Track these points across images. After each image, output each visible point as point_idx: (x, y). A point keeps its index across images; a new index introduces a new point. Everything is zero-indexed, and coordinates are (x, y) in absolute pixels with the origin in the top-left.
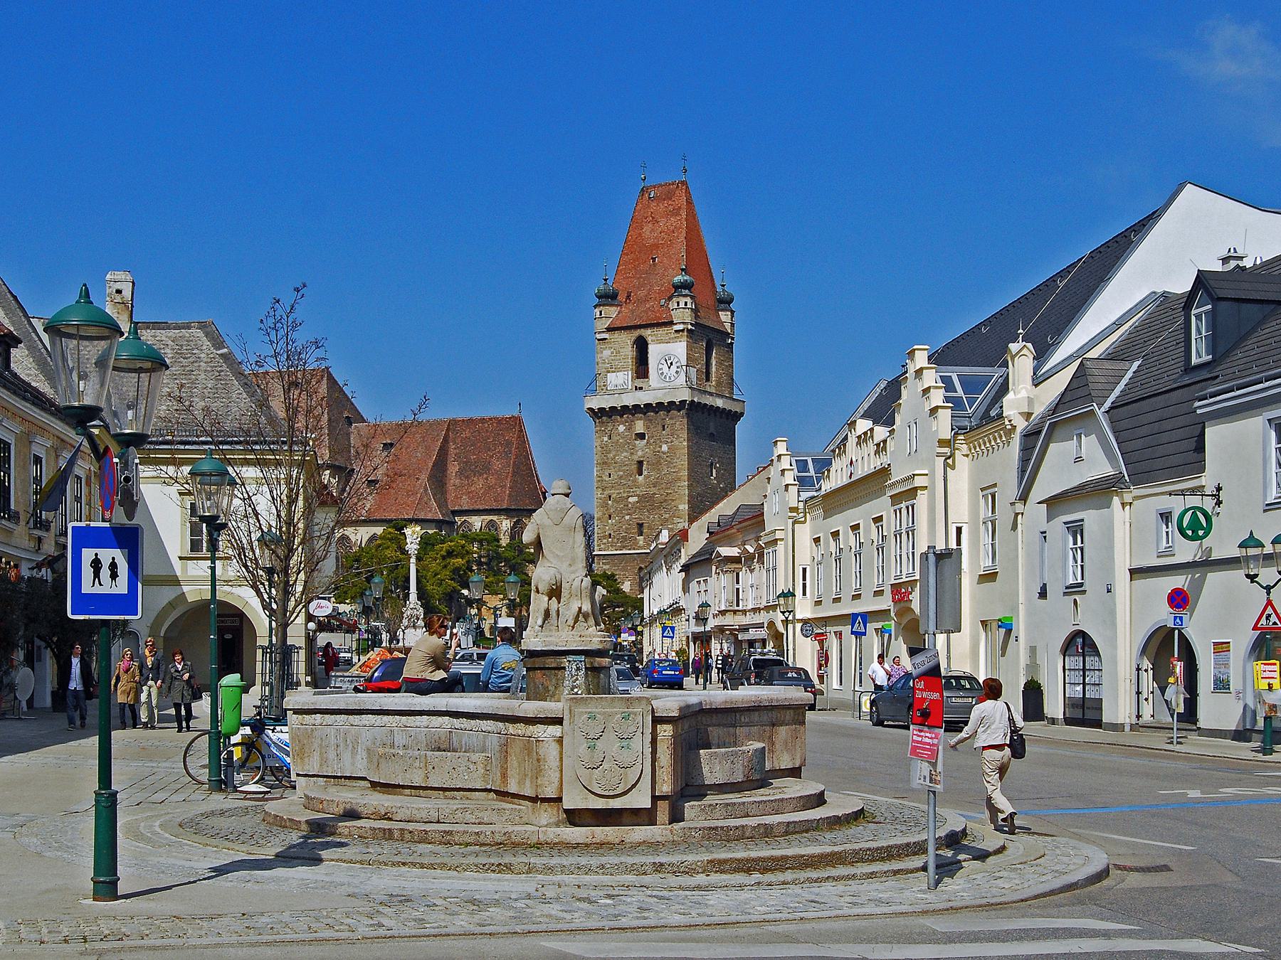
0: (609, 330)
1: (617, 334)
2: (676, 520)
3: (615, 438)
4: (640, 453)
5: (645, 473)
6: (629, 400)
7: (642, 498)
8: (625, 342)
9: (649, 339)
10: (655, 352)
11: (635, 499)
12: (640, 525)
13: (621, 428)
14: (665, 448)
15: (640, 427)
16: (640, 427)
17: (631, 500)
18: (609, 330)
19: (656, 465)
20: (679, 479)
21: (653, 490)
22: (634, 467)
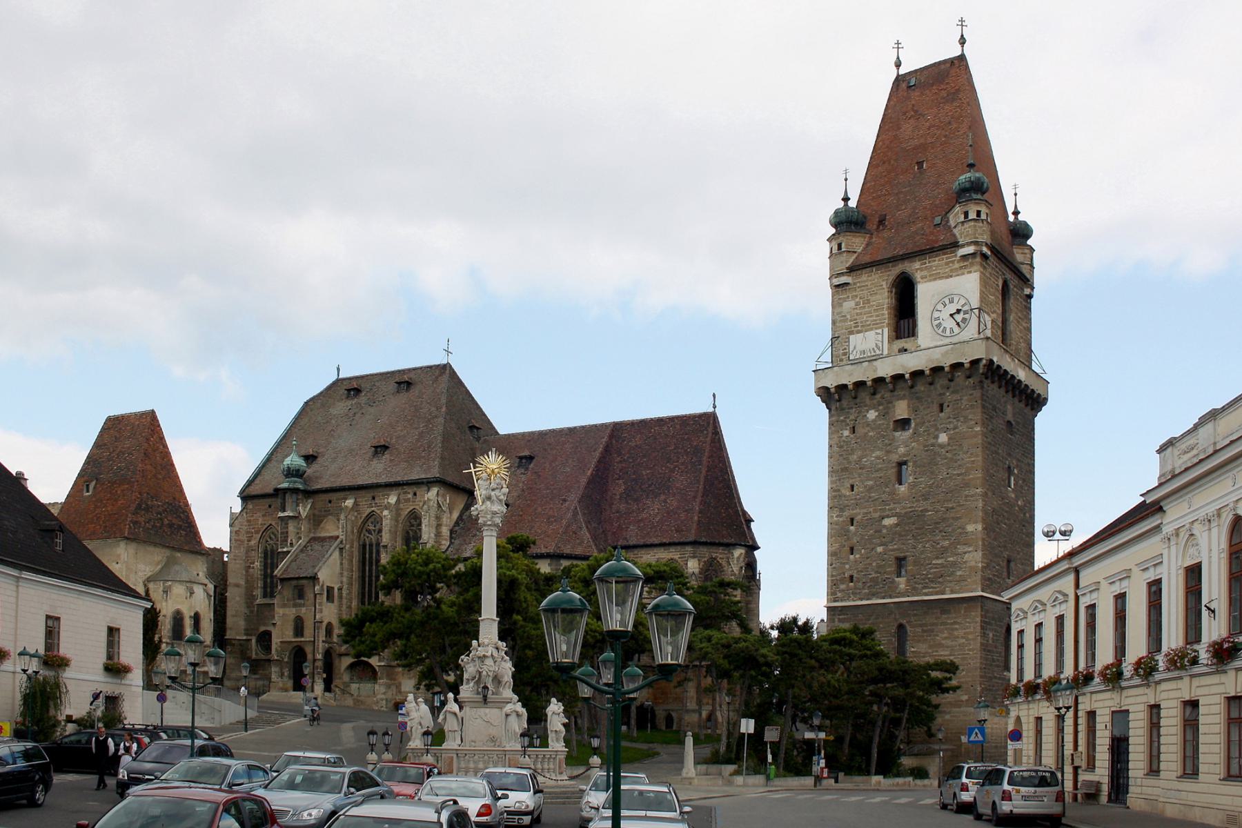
2: (961, 549)
3: (860, 431)
4: (902, 450)
6: (886, 369)
7: (904, 519)
10: (926, 294)
13: (872, 415)
15: (901, 409)
17: (887, 522)
18: (852, 270)
20: (967, 485)
22: (892, 472)
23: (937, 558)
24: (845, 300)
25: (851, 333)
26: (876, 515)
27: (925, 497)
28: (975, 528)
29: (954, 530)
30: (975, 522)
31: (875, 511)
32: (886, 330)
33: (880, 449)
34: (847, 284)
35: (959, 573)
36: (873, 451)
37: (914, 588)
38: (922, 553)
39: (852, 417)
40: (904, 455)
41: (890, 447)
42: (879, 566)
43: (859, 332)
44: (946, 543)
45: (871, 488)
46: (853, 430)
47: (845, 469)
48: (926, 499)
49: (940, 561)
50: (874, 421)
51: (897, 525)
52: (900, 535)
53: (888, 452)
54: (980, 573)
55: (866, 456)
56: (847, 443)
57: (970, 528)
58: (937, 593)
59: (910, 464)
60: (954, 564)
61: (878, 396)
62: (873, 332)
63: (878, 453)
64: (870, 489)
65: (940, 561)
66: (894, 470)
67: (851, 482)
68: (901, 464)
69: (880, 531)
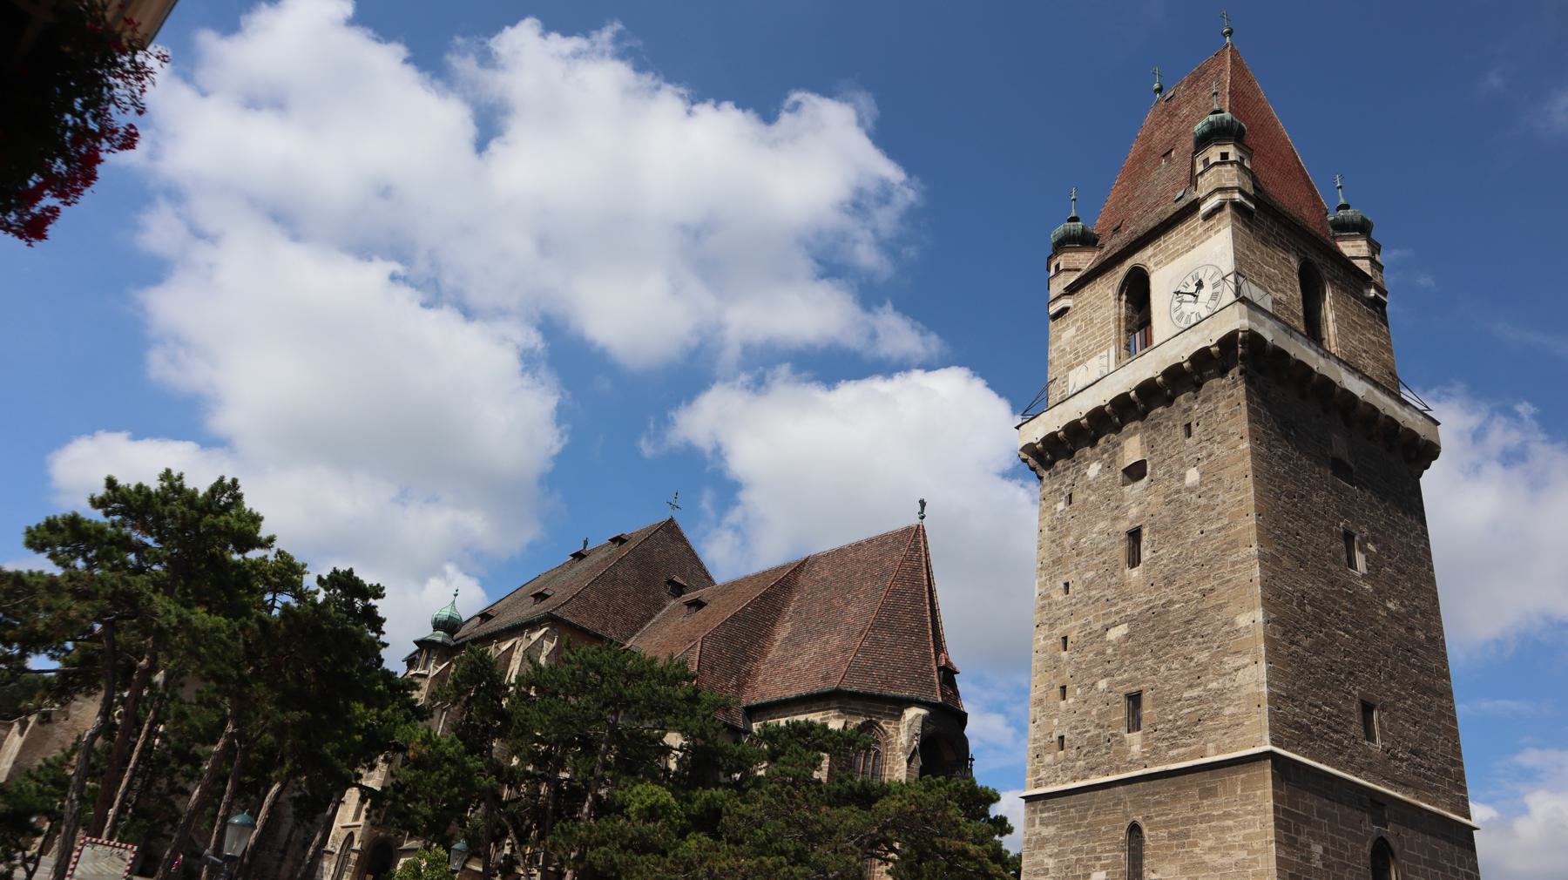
0: (1071, 290)
1: (1087, 293)
2: (1231, 662)
3: (1078, 497)
4: (1134, 511)
5: (1146, 555)
8: (1105, 298)
9: (1151, 266)
11: (1122, 630)
12: (1135, 700)
13: (1094, 470)
14: (1192, 476)
16: (1132, 449)
17: (1115, 634)
18: (1071, 290)
19: (1172, 529)
20: (1233, 545)
21: (1171, 593)
22: (1121, 550)
23: (1191, 686)
24: (1064, 330)
25: (1071, 368)
26: (1098, 626)
27: (1169, 582)
28: (1252, 619)
29: (1216, 631)
31: (1097, 619)
33: (1104, 518)
34: (1065, 310)
35: (1227, 711)
36: (1094, 524)
37: (1155, 750)
38: (1166, 680)
39: (1068, 481)
40: (1139, 518)
41: (1118, 512)
42: (1101, 715)
44: (1204, 657)
45: (1092, 582)
47: (1057, 561)
48: (1170, 583)
49: (1195, 693)
51: (1128, 636)
52: (1134, 654)
53: (1115, 519)
54: (1265, 707)
58: (1192, 756)
59: (1145, 531)
60: (1220, 694)
61: (1101, 441)
62: (1096, 359)
63: (1102, 525)
64: (1089, 585)
65: (1195, 693)
66: (1125, 545)
67: (1065, 578)
68: (1135, 535)
69: (1103, 653)
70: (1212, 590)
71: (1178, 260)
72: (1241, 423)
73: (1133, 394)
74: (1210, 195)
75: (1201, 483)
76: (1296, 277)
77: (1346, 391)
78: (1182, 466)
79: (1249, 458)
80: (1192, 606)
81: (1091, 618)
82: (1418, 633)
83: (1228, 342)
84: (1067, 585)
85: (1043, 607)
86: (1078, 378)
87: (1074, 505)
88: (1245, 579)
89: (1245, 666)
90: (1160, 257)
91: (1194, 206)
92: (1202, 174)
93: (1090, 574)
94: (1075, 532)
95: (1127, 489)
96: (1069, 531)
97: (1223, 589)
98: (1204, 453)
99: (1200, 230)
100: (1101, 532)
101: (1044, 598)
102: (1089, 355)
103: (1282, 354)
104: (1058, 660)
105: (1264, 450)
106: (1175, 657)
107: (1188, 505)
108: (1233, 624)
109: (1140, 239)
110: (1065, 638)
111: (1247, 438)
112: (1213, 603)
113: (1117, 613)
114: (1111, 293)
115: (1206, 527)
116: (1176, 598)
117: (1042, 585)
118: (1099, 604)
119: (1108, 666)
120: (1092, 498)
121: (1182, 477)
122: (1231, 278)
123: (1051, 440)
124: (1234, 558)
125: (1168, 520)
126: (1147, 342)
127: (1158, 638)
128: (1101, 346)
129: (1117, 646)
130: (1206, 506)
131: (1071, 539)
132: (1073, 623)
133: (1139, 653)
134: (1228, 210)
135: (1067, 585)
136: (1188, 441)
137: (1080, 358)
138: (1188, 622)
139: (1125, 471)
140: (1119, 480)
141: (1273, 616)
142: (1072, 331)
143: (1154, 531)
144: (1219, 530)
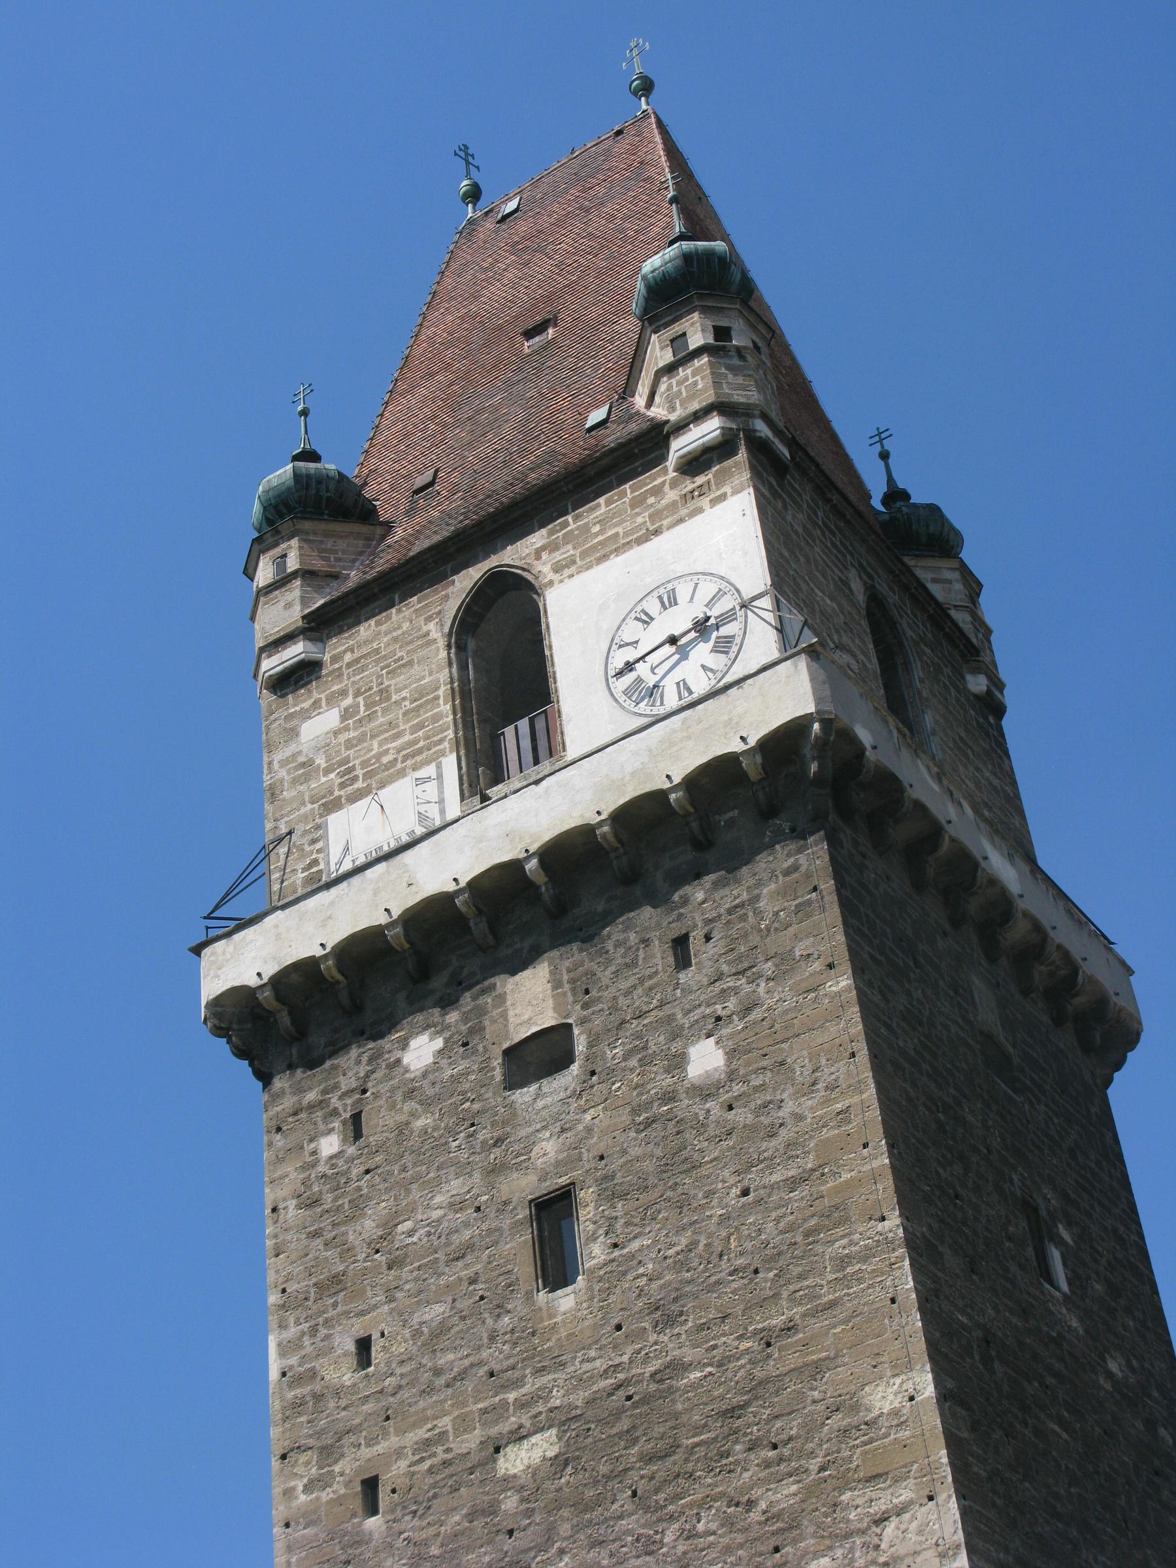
2: (859, 1503)
3: (379, 1123)
4: (548, 1148)
5: (594, 1253)
9: (544, 569)
13: (421, 1051)
14: (705, 1058)
17: (518, 1460)
20: (836, 1216)
21: (674, 1344)
22: (518, 1247)
24: (306, 715)
25: (333, 806)
26: (470, 1441)
27: (666, 1316)
28: (904, 1392)
29: (811, 1428)
30: (904, 1366)
31: (463, 1424)
32: (450, 764)
33: (464, 1170)
36: (436, 1185)
39: (347, 1082)
40: (560, 1165)
43: (354, 798)
44: (786, 1493)
45: (441, 1330)
46: (356, 1127)
50: (435, 1067)
51: (560, 1463)
52: (582, 1506)
53: (495, 1171)
55: (412, 1209)
56: (336, 1179)
57: (884, 1398)
59: (587, 1195)
63: (456, 1186)
67: (358, 1328)
69: (492, 1509)
70: (789, 1328)
71: (617, 563)
72: (825, 934)
73: (532, 865)
74: (698, 417)
75: (731, 1076)
76: (864, 623)
77: (993, 882)
78: (675, 1036)
79: (854, 1012)
80: (739, 1370)
81: (445, 1423)
82: (1162, 1432)
83: (783, 744)
84: (364, 1346)
85: (297, 1406)
86: (354, 831)
87: (372, 1137)
88: (878, 1296)
89: (900, 1511)
90: (568, 551)
91: (652, 442)
92: (670, 369)
93: (438, 1310)
94: (380, 1208)
95: (523, 1096)
96: (358, 1206)
97: (817, 1325)
98: (732, 1004)
99: (671, 495)
100: (456, 1205)
101: (298, 1380)
102: (381, 775)
103: (888, 785)
104: (361, 1540)
105: (877, 998)
106: (705, 1503)
107: (701, 1127)
108: (855, 1408)
109: (514, 505)
110: (371, 1486)
111: (846, 967)
112: (793, 1360)
113: (521, 1405)
114: (437, 632)
115: (752, 1178)
116: (689, 1354)
117: (285, 1350)
118: (469, 1386)
119: (509, 1544)
120: (419, 1123)
121: (679, 1062)
122: (766, 603)
123: (300, 982)
124: (839, 1247)
125: (649, 1166)
126: (546, 747)
127: (649, 1458)
128: (416, 756)
129: (530, 1489)
130: (751, 1129)
131: (369, 1226)
132: (394, 1441)
133: (598, 1502)
134: (742, 455)
135: (364, 1346)
136: (683, 977)
137: (357, 782)
138: (732, 1412)
139: (507, 1053)
140: (498, 1074)
141: (950, 1384)
142: (329, 719)
143: (611, 1194)
144: (793, 1184)
